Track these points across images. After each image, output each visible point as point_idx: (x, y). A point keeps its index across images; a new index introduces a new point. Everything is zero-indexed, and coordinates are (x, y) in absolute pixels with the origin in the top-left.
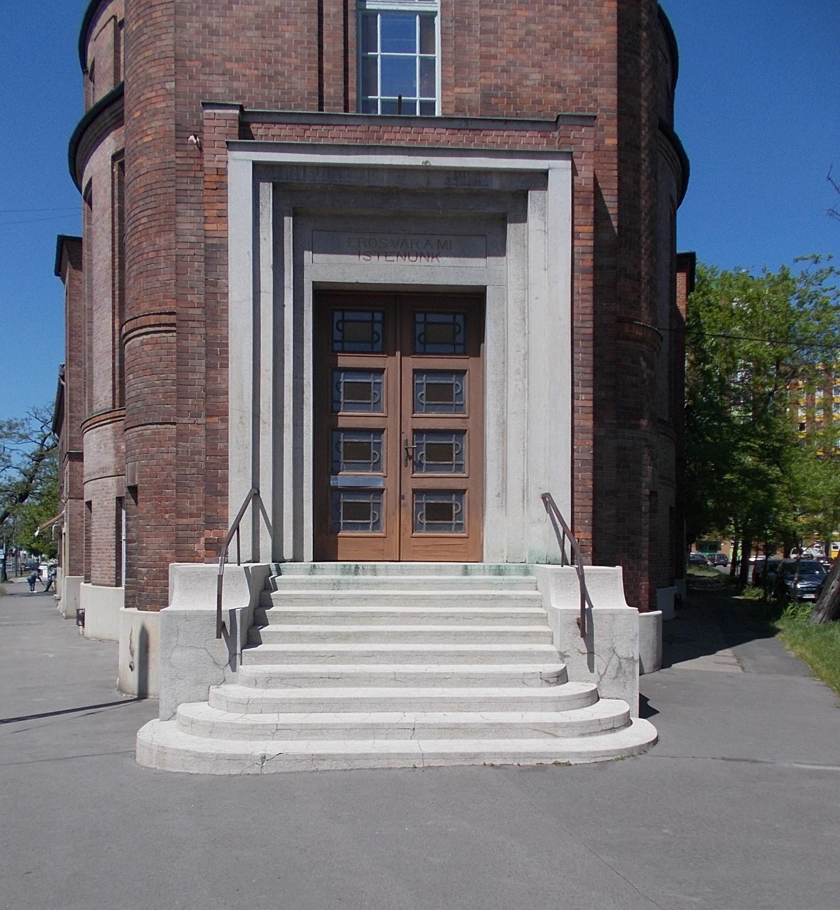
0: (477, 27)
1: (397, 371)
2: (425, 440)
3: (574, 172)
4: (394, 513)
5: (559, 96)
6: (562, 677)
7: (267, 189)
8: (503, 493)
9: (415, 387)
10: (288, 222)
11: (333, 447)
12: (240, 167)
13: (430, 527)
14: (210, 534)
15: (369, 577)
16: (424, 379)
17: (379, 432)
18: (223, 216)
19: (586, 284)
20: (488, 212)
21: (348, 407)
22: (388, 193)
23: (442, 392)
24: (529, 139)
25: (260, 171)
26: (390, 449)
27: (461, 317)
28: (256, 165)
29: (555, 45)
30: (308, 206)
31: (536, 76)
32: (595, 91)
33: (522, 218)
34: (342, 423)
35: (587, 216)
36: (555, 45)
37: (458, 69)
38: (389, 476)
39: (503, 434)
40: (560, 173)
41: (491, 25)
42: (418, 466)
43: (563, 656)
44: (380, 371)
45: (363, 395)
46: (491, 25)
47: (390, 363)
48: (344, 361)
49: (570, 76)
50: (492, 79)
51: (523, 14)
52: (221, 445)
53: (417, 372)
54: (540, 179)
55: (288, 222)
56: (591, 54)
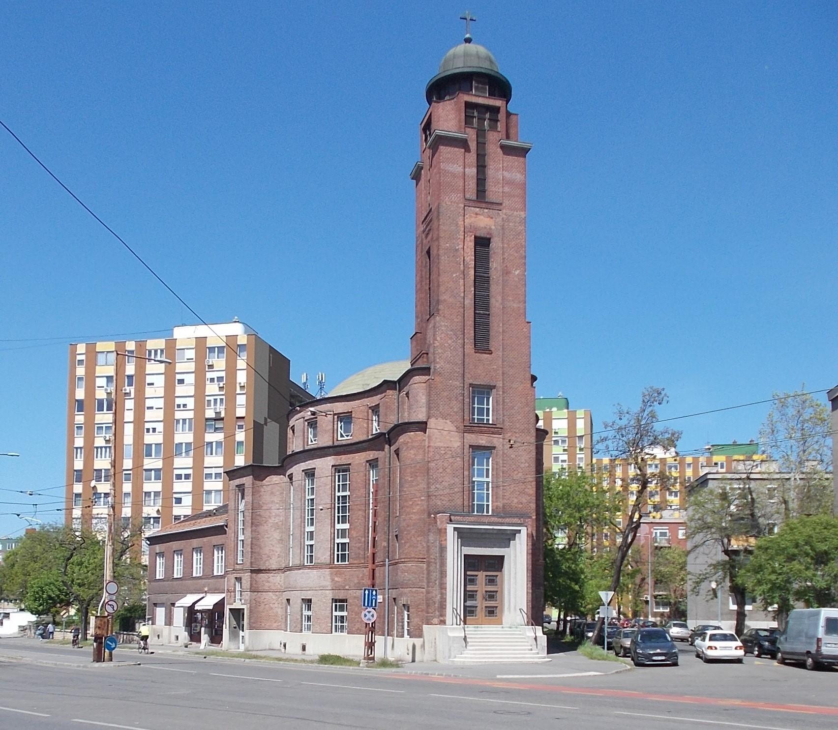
1: (481, 576)
4: (480, 612)
11: (469, 595)
12: (450, 528)
18: (446, 540)
19: (530, 556)
22: (482, 534)
23: (491, 581)
24: (516, 520)
26: (479, 596)
27: (497, 563)
30: (465, 537)
31: (516, 501)
33: (514, 539)
38: (480, 603)
47: (480, 574)
48: (468, 573)
49: (524, 501)
50: (505, 501)
56: (529, 495)
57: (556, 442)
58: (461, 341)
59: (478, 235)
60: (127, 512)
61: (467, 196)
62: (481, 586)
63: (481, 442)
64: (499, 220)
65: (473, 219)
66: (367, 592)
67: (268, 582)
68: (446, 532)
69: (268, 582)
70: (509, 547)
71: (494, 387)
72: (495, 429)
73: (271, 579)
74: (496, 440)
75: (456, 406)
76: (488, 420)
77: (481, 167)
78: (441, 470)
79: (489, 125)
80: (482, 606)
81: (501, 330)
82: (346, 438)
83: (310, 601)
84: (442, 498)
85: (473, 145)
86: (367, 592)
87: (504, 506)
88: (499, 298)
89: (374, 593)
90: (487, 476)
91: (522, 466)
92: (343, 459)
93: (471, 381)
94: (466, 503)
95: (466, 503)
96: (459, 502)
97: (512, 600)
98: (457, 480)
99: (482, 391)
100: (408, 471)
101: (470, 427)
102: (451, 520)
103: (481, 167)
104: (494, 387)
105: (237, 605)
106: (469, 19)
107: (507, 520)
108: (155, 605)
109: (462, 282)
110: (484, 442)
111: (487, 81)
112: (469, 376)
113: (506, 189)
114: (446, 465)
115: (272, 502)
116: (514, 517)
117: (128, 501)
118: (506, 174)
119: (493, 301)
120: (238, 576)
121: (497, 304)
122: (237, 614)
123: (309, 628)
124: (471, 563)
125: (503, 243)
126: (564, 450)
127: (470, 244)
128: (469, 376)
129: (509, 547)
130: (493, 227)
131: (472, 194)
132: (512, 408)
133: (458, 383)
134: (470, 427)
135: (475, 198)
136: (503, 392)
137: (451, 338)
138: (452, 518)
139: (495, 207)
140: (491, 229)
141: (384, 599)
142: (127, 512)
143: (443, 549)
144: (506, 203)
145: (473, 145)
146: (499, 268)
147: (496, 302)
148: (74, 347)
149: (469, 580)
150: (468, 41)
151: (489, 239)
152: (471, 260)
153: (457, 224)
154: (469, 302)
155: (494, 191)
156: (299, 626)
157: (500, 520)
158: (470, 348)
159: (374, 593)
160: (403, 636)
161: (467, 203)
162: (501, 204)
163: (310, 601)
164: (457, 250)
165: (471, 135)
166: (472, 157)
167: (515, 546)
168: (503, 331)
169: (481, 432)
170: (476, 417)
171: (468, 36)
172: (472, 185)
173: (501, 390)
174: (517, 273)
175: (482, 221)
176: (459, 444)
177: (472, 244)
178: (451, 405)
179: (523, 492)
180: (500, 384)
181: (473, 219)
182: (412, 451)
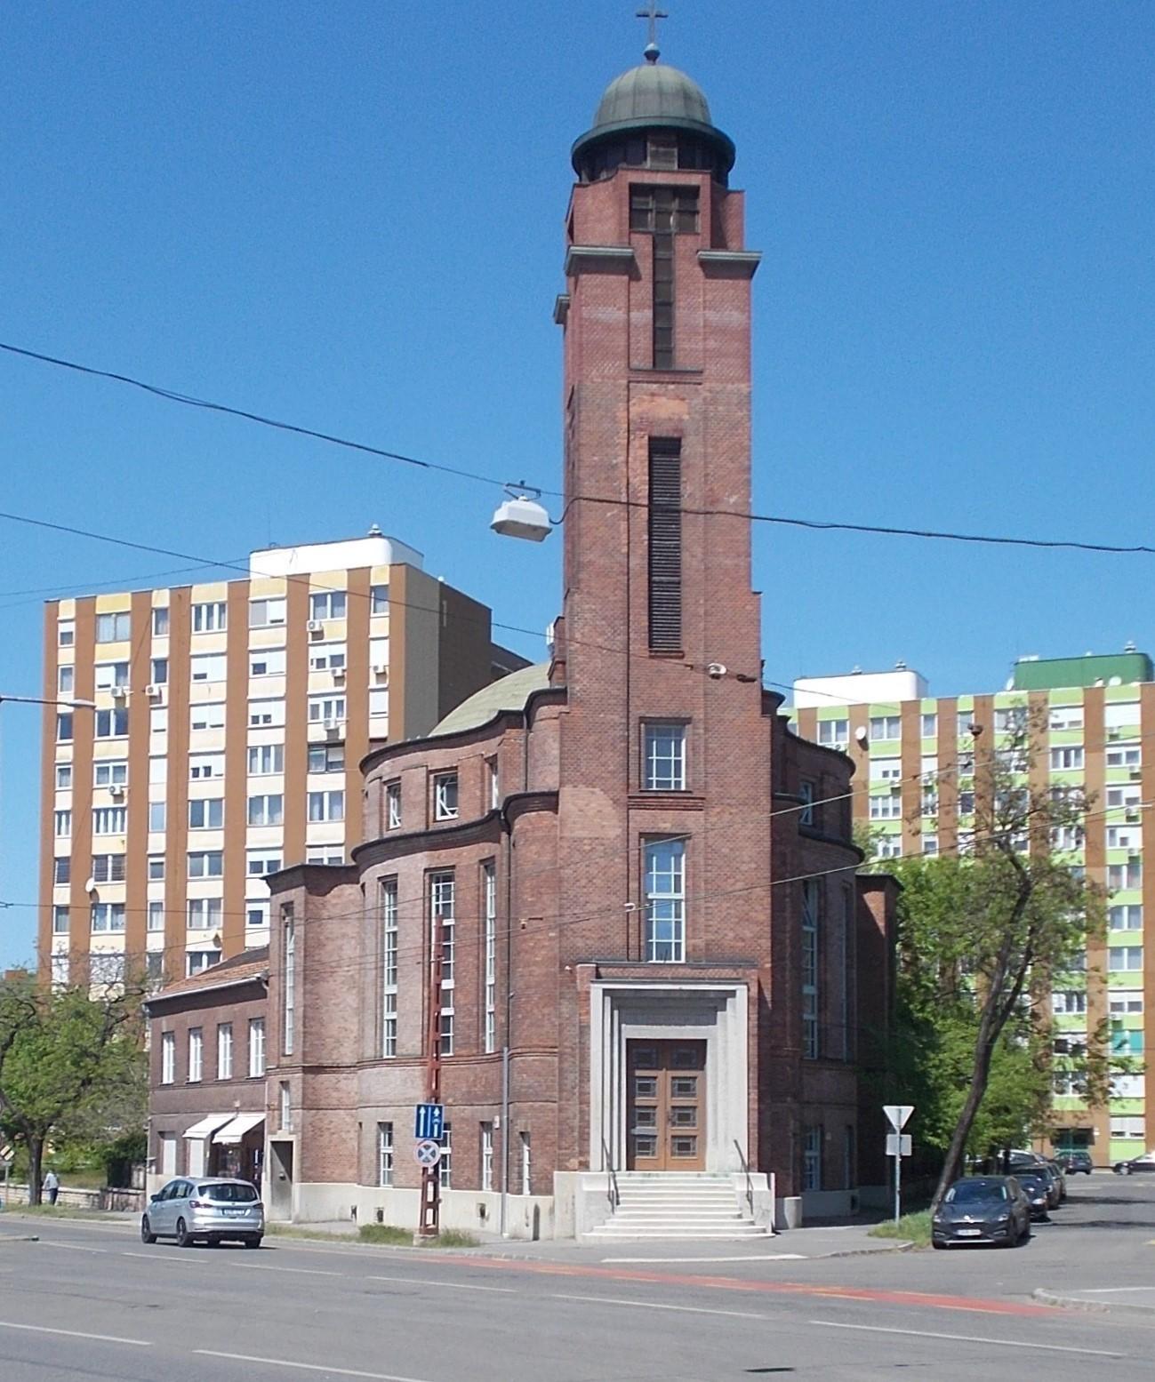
0: (703, 911)
1: (664, 1078)
2: (677, 1111)
3: (749, 990)
4: (662, 1148)
5: (743, 944)
6: (740, 1216)
7: (608, 999)
8: (715, 1138)
9: (673, 1086)
10: (616, 1012)
11: (636, 1115)
12: (596, 991)
13: (680, 1155)
14: (582, 1159)
15: (655, 1178)
16: (677, 1082)
17: (655, 1107)
18: (588, 1013)
19: (754, 1041)
20: (709, 1007)
21: (640, 1095)
23: (684, 1088)
25: (606, 992)
26: (660, 1116)
27: (694, 1054)
28: (604, 990)
29: (741, 920)
30: (626, 1006)
31: (731, 935)
32: (759, 941)
33: (724, 1009)
34: (637, 1104)
35: (754, 1010)
36: (741, 920)
37: (694, 930)
38: (660, 1129)
39: (715, 1111)
40: (742, 991)
41: (710, 911)
42: (674, 1124)
43: (741, 1209)
44: (655, 1078)
45: (646, 1089)
46: (710, 911)
47: (660, 1074)
48: (638, 1073)
49: (748, 934)
51: (725, 905)
52: (587, 1118)
53: (673, 1078)
54: (733, 993)
55: (616, 1012)
56: (758, 923)
57: (1114, 759)
58: (623, 638)
59: (655, 434)
60: (156, 942)
61: (635, 363)
62: (663, 1097)
63: (663, 825)
64: (697, 401)
65: (645, 406)
66: (422, 1111)
67: (337, 1090)
68: (588, 999)
69: (337, 1090)
70: (715, 1023)
71: (688, 721)
72: (689, 801)
73: (342, 1085)
74: (692, 821)
75: (614, 760)
76: (678, 784)
77: (663, 307)
78: (583, 882)
79: (679, 224)
80: (659, 1130)
81: (701, 611)
82: (450, 816)
83: (390, 1126)
84: (587, 934)
85: (645, 267)
86: (422, 1111)
87: (707, 945)
88: (698, 551)
89: (437, 1112)
90: (677, 890)
91: (744, 867)
92: (443, 857)
93: (642, 712)
94: (633, 942)
95: (633, 942)
96: (619, 940)
97: (721, 1123)
98: (613, 898)
99: (667, 728)
100: (528, 884)
101: (640, 799)
102: (598, 976)
103: (663, 307)
104: (688, 721)
105: (283, 1136)
106: (652, 16)
107: (711, 973)
108: (162, 1134)
109: (623, 525)
110: (668, 825)
111: (674, 138)
112: (639, 703)
113: (712, 344)
114: (593, 871)
115: (344, 935)
116: (723, 967)
117: (159, 921)
118: (712, 316)
119: (685, 557)
120: (285, 1078)
121: (695, 563)
122: (284, 1149)
123: (390, 1181)
124: (641, 1055)
125: (705, 446)
126: (1134, 776)
127: (640, 452)
128: (639, 703)
129: (715, 1023)
130: (686, 417)
131: (643, 359)
132: (724, 759)
133: (618, 718)
134: (640, 799)
135: (649, 366)
136: (706, 730)
137: (603, 633)
138: (602, 970)
139: (688, 378)
140: (681, 420)
141: (501, 1122)
142: (156, 942)
143: (584, 1030)
144: (712, 369)
145: (645, 267)
146: (698, 495)
147: (691, 559)
148: (53, 606)
149: (635, 1087)
150: (652, 56)
151: (679, 440)
152: (642, 483)
153: (614, 420)
154: (639, 562)
155: (687, 349)
156: (374, 1174)
157: (696, 973)
158: (639, 647)
159: (437, 1112)
160: (520, 1192)
161: (634, 377)
163: (390, 1126)
164: (614, 467)
165: (642, 246)
166: (643, 290)
167: (725, 1021)
168: (706, 613)
169: (663, 808)
170: (654, 778)
171: (651, 47)
172: (643, 342)
173: (701, 725)
174: (732, 500)
175: (665, 407)
176: (619, 831)
177: (644, 453)
178: (603, 760)
179: (745, 919)
180: (699, 715)
181: (645, 406)
182: (533, 847)
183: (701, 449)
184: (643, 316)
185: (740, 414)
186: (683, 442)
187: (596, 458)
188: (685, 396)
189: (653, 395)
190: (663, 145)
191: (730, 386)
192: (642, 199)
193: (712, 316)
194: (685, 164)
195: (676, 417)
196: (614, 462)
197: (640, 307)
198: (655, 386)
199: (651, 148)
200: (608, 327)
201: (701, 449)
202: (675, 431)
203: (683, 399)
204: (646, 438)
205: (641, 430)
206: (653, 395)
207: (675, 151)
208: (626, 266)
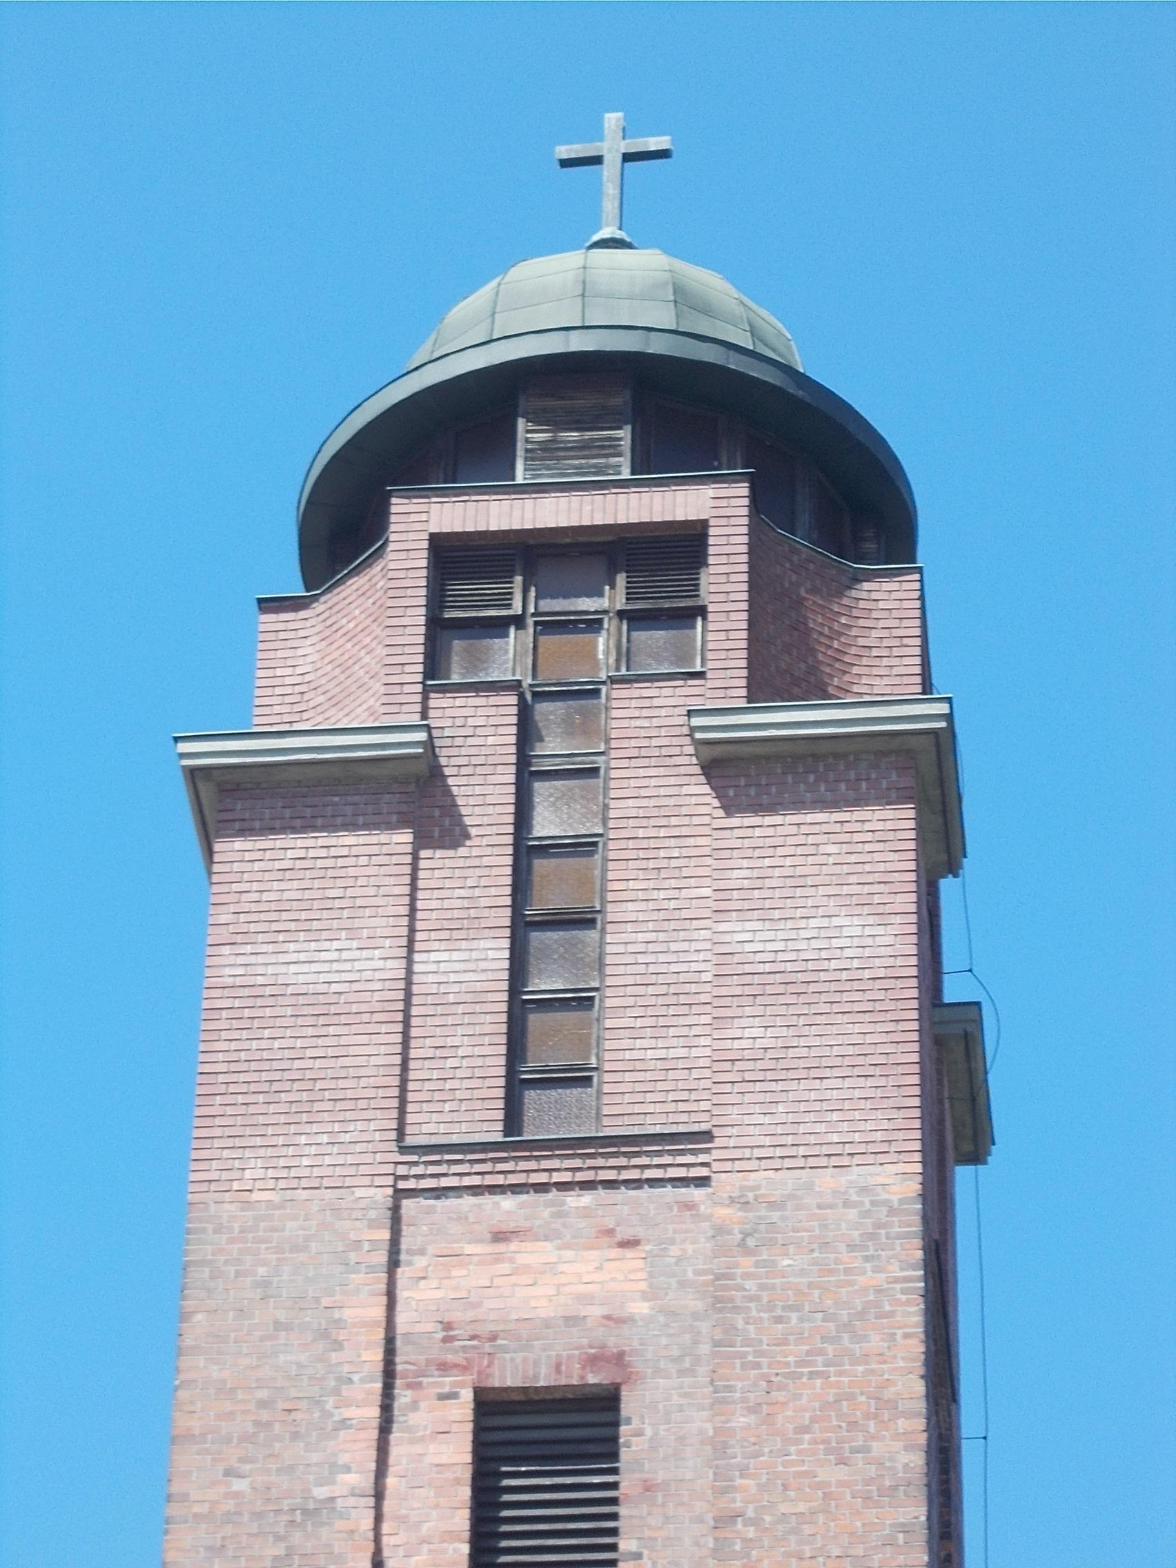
59: (509, 1374)
61: (427, 1126)
65: (469, 1279)
77: (548, 910)
85: (483, 796)
103: (548, 910)
111: (621, 400)
113: (751, 1032)
118: (743, 934)
125: (720, 1402)
127: (438, 1446)
130: (641, 1308)
139: (652, 1164)
144: (745, 1123)
145: (483, 796)
153: (329, 1336)
155: (642, 1066)
161: (423, 1173)
162: (707, 1136)
164: (314, 1513)
165: (476, 739)
166: (474, 876)
177: (457, 1452)
181: (469, 1279)
183: (700, 1422)
184: (467, 965)
185: (869, 1278)
186: (628, 1406)
187: (239, 1485)
188: (639, 1232)
189: (500, 1237)
190: (579, 426)
191: (827, 1181)
192: (489, 588)
193: (748, 936)
194: (659, 459)
195: (597, 1311)
196: (321, 1492)
197: (459, 930)
198: (508, 1202)
199: (527, 433)
200: (322, 1010)
201: (700, 1422)
202: (592, 1361)
203: (630, 1244)
204: (467, 1395)
205: (444, 1367)
206: (500, 1237)
207: (624, 434)
208: (413, 795)
